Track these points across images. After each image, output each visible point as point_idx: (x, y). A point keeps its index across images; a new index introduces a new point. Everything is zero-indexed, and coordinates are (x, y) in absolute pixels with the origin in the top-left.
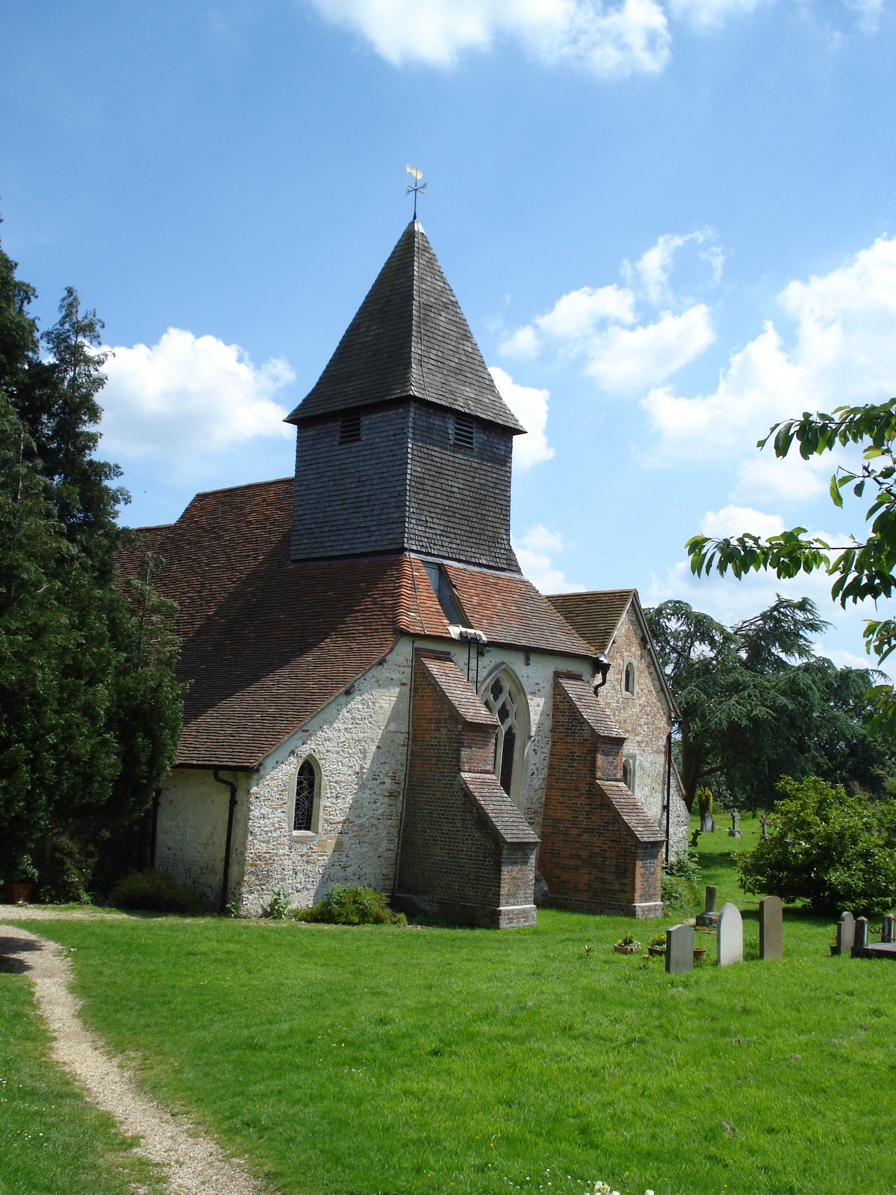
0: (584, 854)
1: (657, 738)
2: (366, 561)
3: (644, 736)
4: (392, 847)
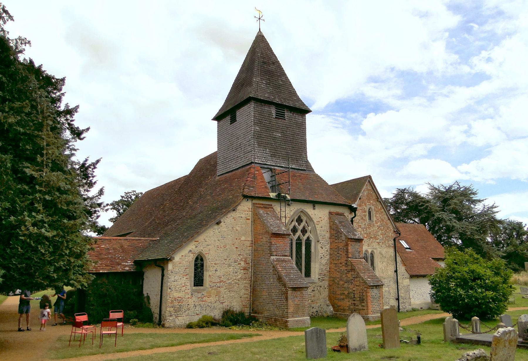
0: (346, 293)
1: (388, 241)
2: (240, 170)
3: (381, 240)
4: (247, 292)
